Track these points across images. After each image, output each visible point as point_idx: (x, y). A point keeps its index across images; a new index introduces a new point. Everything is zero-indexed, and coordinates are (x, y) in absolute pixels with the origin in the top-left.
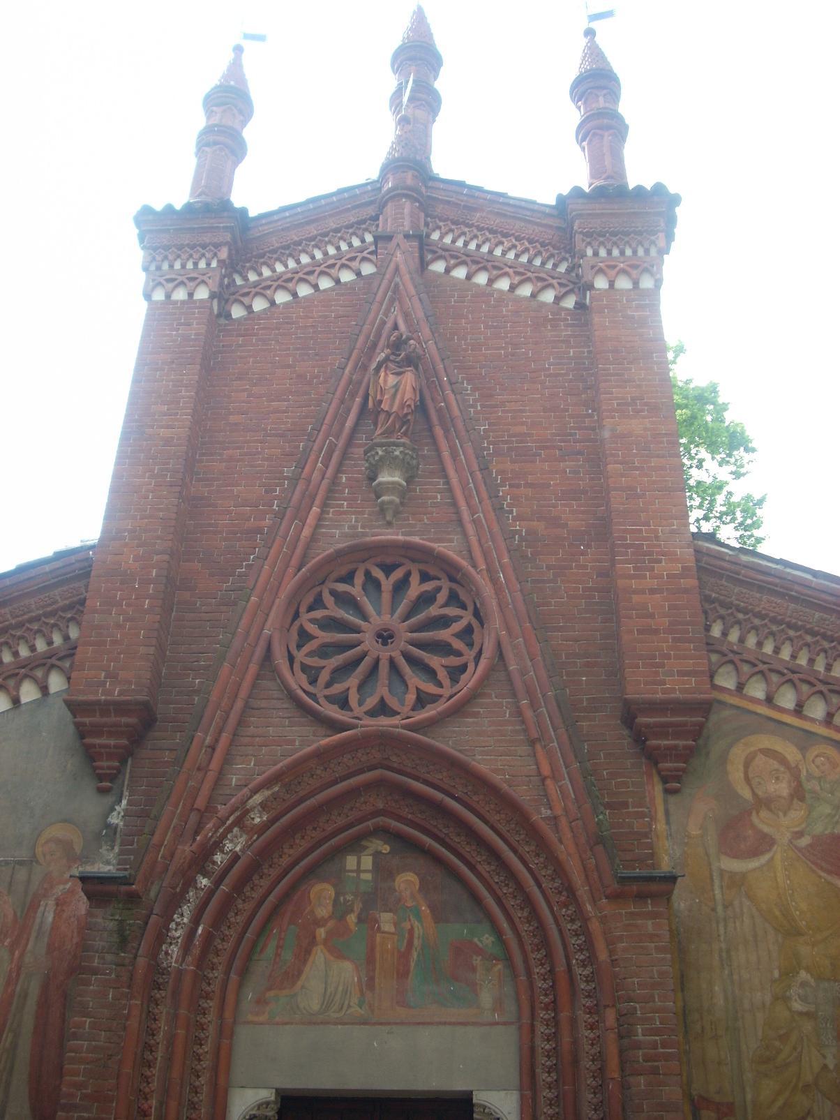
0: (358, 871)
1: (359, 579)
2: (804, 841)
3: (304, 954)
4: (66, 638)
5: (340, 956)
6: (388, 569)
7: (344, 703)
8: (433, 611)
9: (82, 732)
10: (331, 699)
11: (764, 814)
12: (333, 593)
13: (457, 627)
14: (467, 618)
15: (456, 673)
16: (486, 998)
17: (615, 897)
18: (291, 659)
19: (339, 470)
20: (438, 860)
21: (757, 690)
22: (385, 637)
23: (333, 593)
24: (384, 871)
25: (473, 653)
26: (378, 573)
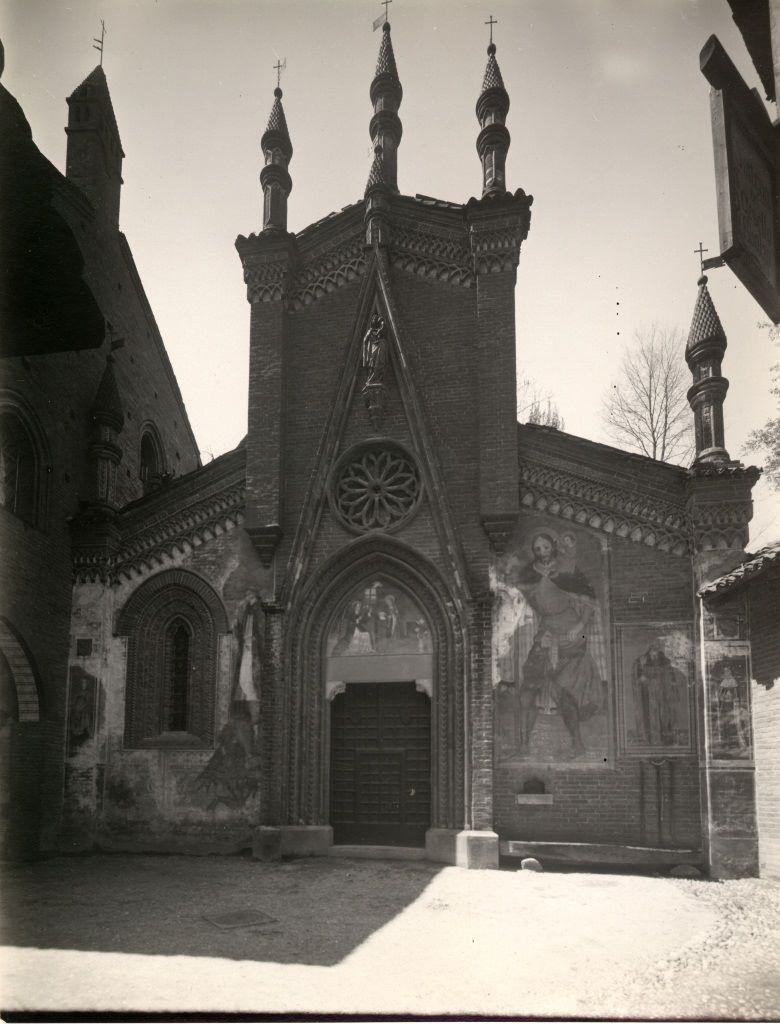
1: (364, 461)
2: (557, 575)
3: (350, 631)
4: (242, 498)
5: (362, 630)
6: (377, 455)
7: (359, 522)
8: (398, 475)
9: (254, 542)
10: (355, 521)
11: (540, 564)
12: (353, 469)
13: (407, 483)
14: (413, 478)
15: (407, 505)
16: (421, 645)
18: (337, 503)
19: (351, 404)
20: (400, 588)
21: (542, 504)
22: (377, 489)
23: (353, 469)
24: (381, 594)
25: (415, 494)
26: (373, 457)
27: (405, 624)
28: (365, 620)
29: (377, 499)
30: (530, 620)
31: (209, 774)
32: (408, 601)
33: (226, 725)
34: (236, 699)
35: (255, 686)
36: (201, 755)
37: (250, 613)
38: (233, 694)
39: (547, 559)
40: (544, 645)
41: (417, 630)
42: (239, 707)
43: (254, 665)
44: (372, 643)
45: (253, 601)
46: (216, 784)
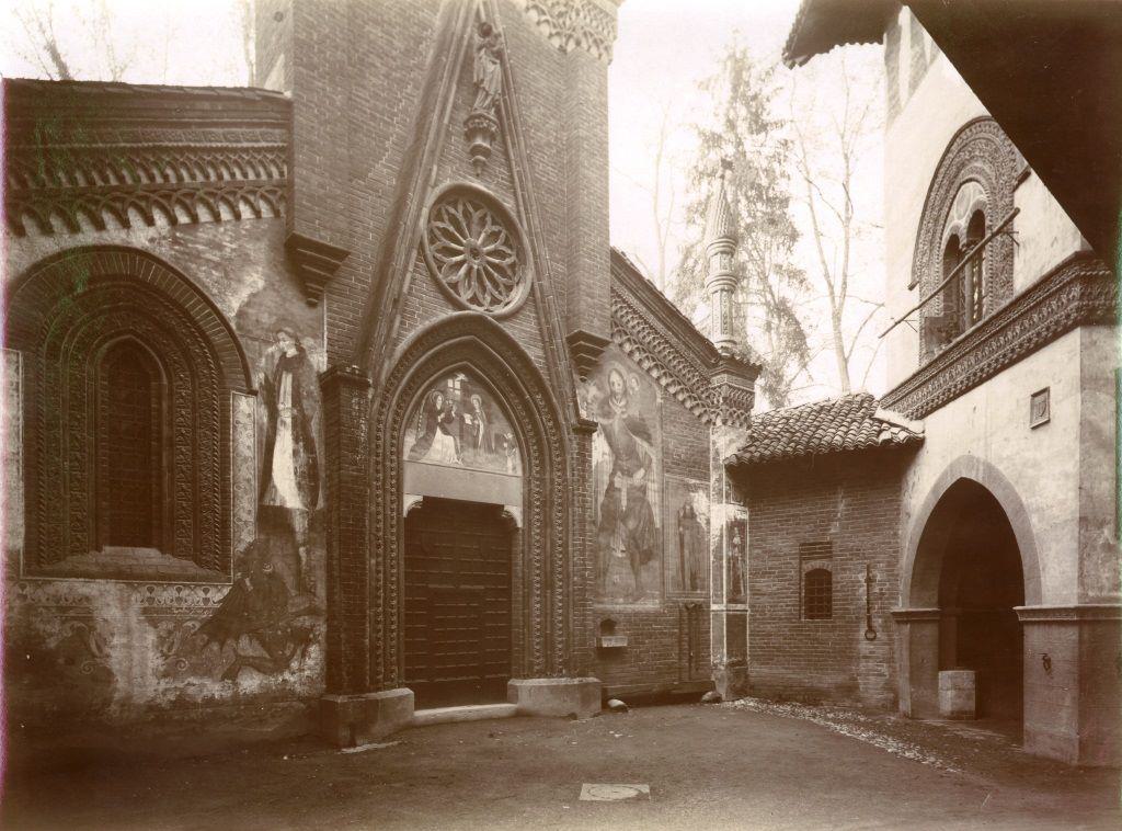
0: (455, 389)
3: (431, 431)
5: (446, 432)
17: (576, 431)
27: (493, 437)
28: (448, 419)
29: (476, 267)
30: (606, 457)
31: (220, 626)
32: (495, 407)
33: (251, 544)
34: (267, 502)
35: (300, 486)
36: (206, 591)
37: (288, 371)
38: (262, 496)
39: (619, 396)
40: (616, 485)
41: (505, 445)
42: (272, 518)
43: (295, 453)
44: (457, 452)
45: (291, 352)
46: (237, 639)
